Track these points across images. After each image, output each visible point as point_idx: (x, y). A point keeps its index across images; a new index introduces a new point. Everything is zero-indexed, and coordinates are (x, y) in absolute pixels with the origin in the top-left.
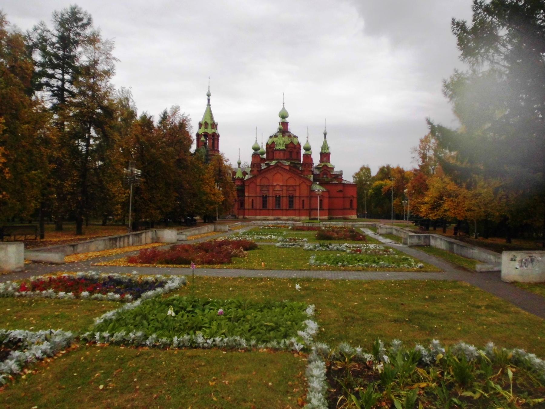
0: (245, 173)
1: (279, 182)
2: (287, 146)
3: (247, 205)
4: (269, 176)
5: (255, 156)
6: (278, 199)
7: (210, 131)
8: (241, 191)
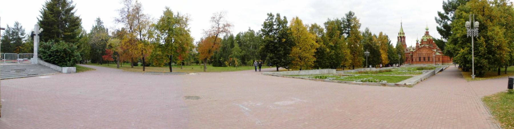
0: (414, 49)
1: (424, 53)
2: (428, 40)
3: (414, 60)
4: (421, 50)
5: (417, 43)
6: (424, 58)
7: (402, 36)
8: (412, 56)
